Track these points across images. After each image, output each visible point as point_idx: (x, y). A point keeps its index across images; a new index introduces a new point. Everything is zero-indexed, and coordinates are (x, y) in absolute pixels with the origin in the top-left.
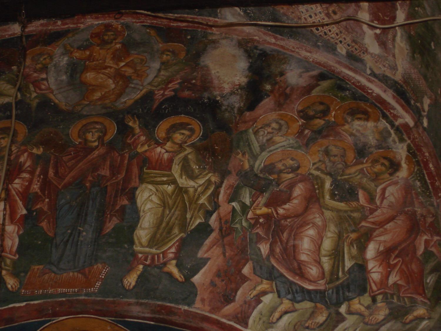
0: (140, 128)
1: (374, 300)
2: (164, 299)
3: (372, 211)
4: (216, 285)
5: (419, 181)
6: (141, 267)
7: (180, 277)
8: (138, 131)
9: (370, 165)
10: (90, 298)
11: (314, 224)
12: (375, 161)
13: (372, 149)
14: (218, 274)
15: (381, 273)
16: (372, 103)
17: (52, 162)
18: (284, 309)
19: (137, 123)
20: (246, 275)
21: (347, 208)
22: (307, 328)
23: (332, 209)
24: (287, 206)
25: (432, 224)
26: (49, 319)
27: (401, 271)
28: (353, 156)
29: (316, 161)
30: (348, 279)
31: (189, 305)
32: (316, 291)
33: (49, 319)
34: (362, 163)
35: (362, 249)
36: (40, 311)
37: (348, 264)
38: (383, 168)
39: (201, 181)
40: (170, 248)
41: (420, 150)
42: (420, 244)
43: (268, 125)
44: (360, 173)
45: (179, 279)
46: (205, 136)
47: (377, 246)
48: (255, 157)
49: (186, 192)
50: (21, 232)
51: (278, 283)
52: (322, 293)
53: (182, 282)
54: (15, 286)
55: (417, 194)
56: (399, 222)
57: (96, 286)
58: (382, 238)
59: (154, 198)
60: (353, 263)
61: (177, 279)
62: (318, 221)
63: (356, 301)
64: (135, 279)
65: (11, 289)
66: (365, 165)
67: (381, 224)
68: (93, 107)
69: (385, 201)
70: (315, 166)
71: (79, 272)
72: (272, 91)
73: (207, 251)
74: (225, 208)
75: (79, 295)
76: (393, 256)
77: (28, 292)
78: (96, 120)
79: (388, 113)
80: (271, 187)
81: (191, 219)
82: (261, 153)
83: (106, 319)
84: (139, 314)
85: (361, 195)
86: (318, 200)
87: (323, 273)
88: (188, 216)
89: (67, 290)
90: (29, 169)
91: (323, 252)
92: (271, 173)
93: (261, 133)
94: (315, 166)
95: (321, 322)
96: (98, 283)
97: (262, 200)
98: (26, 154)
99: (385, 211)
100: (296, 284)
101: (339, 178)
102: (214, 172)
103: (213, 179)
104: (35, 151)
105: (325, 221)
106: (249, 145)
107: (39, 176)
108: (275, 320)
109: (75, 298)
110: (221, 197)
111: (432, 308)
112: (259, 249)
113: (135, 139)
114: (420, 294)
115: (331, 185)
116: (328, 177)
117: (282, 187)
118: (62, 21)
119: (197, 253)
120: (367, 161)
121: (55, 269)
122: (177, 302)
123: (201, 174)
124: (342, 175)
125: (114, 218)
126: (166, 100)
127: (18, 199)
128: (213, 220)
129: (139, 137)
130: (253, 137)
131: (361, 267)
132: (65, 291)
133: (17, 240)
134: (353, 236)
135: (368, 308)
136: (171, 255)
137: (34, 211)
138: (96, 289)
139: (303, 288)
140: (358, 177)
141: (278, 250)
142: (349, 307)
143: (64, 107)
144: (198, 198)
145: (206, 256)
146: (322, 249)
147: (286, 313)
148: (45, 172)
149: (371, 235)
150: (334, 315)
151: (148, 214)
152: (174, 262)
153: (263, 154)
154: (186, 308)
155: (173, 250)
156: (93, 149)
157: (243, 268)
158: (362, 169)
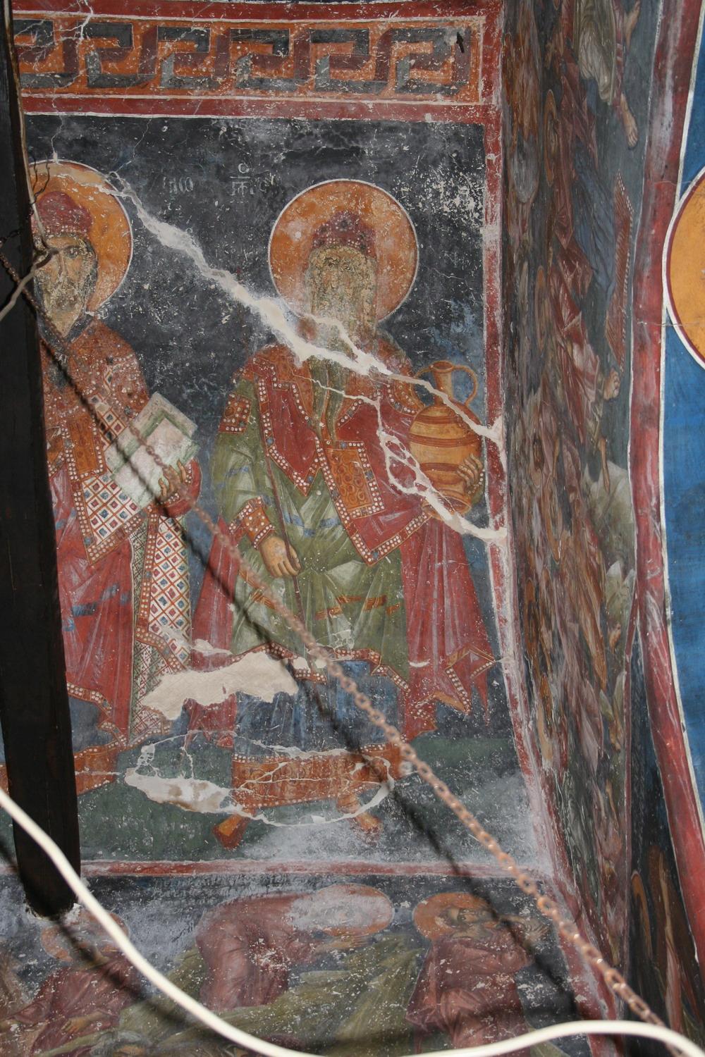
26: (663, 330)
33: (663, 330)
83: (678, 204)
84: (666, 124)
118: (489, 151)
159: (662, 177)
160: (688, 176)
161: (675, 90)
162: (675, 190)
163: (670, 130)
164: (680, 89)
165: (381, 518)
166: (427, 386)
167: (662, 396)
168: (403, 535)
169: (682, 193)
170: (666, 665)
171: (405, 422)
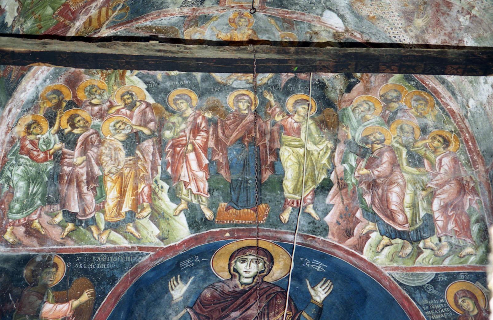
0: (275, 101)
1: (440, 240)
3: (435, 175)
4: (340, 224)
5: (463, 155)
6: (291, 208)
8: (273, 103)
9: (431, 141)
11: (398, 184)
12: (434, 138)
13: (431, 129)
14: (341, 216)
15: (443, 221)
16: (429, 92)
17: (219, 124)
18: (384, 243)
19: (272, 97)
21: (418, 173)
22: (400, 257)
23: (408, 173)
24: (379, 169)
25: (473, 187)
27: (456, 221)
28: (419, 134)
29: (396, 135)
30: (422, 225)
31: (324, 236)
32: (403, 232)
34: (425, 139)
35: (430, 203)
37: (422, 214)
38: (439, 144)
39: (321, 147)
40: (307, 195)
41: (462, 132)
42: (466, 202)
43: (361, 105)
44: (424, 146)
45: (316, 218)
46: (319, 111)
47: (439, 202)
48: (355, 130)
49: (312, 154)
50: (208, 178)
52: (408, 232)
55: (462, 165)
56: (452, 185)
58: (442, 196)
59: (291, 157)
60: (425, 213)
62: (400, 181)
63: (428, 240)
64: (288, 217)
66: (428, 141)
67: (441, 186)
68: (239, 82)
69: (442, 168)
70: (396, 140)
71: (251, 209)
72: (361, 79)
73: (331, 200)
74: (340, 168)
76: (450, 210)
78: (244, 92)
79: (440, 101)
80: (368, 154)
81: (318, 174)
82: (359, 127)
85: (426, 162)
86: (399, 165)
87: (407, 218)
88: (316, 173)
90: (204, 129)
91: (406, 205)
92: (367, 143)
93: (357, 111)
94: (396, 140)
95: (408, 253)
97: (363, 163)
98: (201, 117)
99: (443, 176)
100: (390, 226)
101: (411, 150)
102: (329, 141)
103: (329, 145)
104: (206, 115)
105: (404, 181)
106: (350, 120)
107: (213, 135)
108: (379, 250)
110: (336, 159)
111: (477, 248)
112: (365, 200)
113: (273, 111)
114: (469, 238)
115: (407, 155)
116: (404, 149)
117: (375, 154)
119: (325, 200)
120: (428, 138)
121: (235, 206)
123: (320, 141)
124: (413, 148)
125: (268, 171)
126: (290, 80)
127: (201, 151)
128: (333, 177)
129: (275, 108)
130: (351, 114)
131: (430, 217)
133: (207, 184)
134: (424, 193)
135: (437, 245)
136: (309, 201)
137: (213, 162)
139: (395, 229)
140: (424, 150)
141: (377, 201)
142: (425, 244)
143: (220, 80)
144: (321, 160)
145: (331, 203)
146: (404, 201)
147: (387, 245)
148: (216, 132)
149: (435, 194)
150: (415, 248)
151: (290, 169)
152: (311, 206)
153: (360, 127)
154: (323, 238)
155: (309, 197)
156: (245, 116)
157: (355, 213)
158: (426, 144)
165: (70, 12)
166: (120, 7)
168: (64, 21)
171: (106, 5)
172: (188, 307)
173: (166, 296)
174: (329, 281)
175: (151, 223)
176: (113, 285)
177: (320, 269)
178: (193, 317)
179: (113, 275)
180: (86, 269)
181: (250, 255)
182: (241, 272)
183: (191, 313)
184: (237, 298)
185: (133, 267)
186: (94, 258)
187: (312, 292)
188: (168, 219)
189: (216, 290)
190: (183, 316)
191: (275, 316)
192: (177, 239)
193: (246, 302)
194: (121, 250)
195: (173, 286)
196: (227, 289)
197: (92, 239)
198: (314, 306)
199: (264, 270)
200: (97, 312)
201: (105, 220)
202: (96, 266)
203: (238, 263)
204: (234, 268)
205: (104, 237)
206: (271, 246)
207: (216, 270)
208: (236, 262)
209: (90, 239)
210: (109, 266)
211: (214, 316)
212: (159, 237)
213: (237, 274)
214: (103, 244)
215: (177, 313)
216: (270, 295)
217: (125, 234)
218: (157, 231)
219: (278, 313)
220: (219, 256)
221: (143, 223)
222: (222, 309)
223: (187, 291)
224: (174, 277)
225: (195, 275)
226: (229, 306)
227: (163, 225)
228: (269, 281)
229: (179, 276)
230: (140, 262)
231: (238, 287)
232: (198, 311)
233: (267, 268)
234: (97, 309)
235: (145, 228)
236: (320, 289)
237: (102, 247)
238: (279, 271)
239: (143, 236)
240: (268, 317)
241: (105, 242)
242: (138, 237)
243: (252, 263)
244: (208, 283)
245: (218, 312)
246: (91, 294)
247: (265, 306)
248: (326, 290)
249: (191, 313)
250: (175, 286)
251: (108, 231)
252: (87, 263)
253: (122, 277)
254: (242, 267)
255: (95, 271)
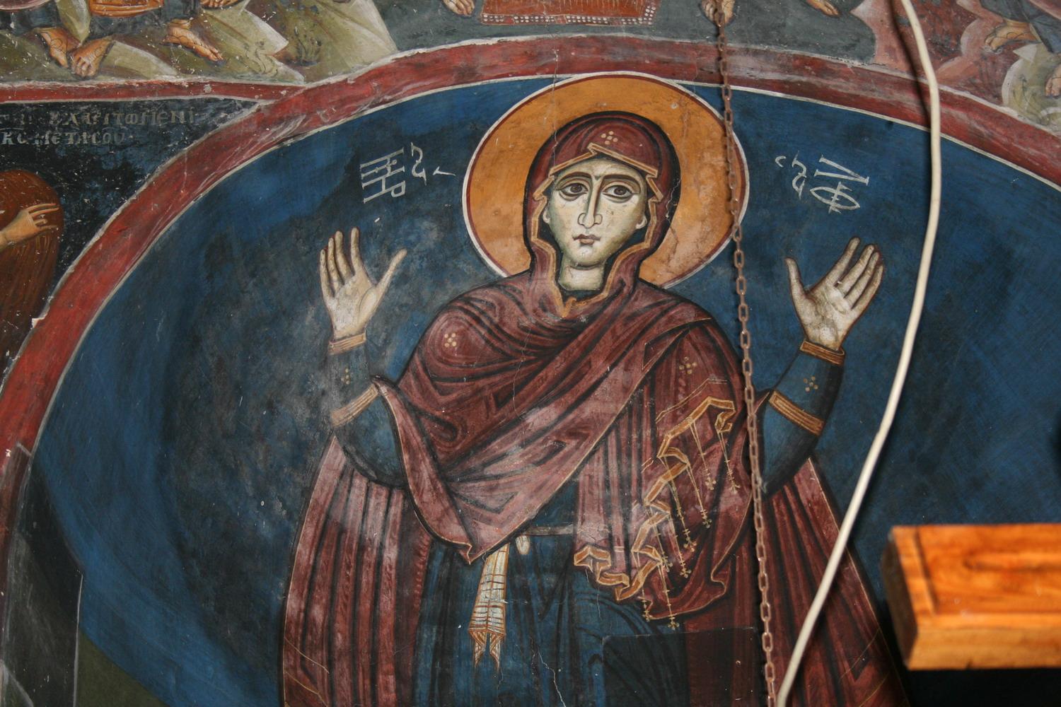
2: (804, 45)
7: (826, 6)
10: (640, 37)
20: (968, 9)
26: (550, 76)
31: (861, 58)
33: (550, 76)
36: (532, 56)
45: (826, 9)
51: (1039, 26)
53: (836, 17)
54: (464, 5)
57: (646, 15)
61: (821, 10)
65: (456, 10)
75: (613, 30)
77: (499, 19)
84: (753, 73)
89: (586, 19)
96: (650, 9)
109: (606, 35)
122: (832, 50)
132: (581, 19)
138: (648, 21)
154: (857, 63)
159: (702, 70)
160: (700, 91)
161: (785, 82)
162: (687, 80)
163: (747, 76)
164: (787, 86)
167: (485, 82)
169: (684, 86)
170: (244, 157)
172: (384, 379)
173: (311, 312)
174: (870, 250)
175: (256, 18)
176: (126, 191)
177: (842, 200)
178: (399, 420)
179: (126, 164)
180: (30, 148)
181: (600, 156)
182: (567, 237)
183: (393, 404)
184: (545, 355)
185: (196, 142)
186: (54, 116)
187: (806, 311)
188: (314, 8)
189: (478, 320)
190: (367, 410)
191: (675, 419)
192: (350, 64)
193: (575, 370)
194: (152, 93)
195: (335, 277)
196: (516, 320)
197: (46, 65)
198: (813, 364)
199: (643, 230)
200: (70, 270)
201: (91, 12)
202: (63, 139)
203: (557, 197)
204: (542, 223)
205: (90, 58)
206: (674, 107)
207: (483, 227)
208: (548, 193)
209: (39, 64)
210: (108, 138)
211: (470, 423)
212: (285, 58)
213: (550, 251)
214: (86, 78)
215: (348, 393)
216: (658, 340)
217: (164, 49)
218: (280, 43)
219: (686, 409)
220: (494, 162)
221: (225, 20)
222: (496, 396)
223: (380, 310)
224: (338, 236)
225: (409, 246)
226: (520, 387)
227: (300, 25)
228: (658, 283)
229: (354, 233)
230: (221, 126)
231: (553, 311)
232: (416, 399)
233: (654, 220)
234: (69, 261)
235: (233, 32)
236: (835, 294)
237: (86, 85)
238: (695, 231)
239: (228, 56)
240: (653, 426)
241: (92, 73)
242: (212, 56)
243: (603, 197)
244: (451, 289)
245: (483, 407)
246: (47, 216)
247: (641, 386)
248: (856, 294)
249: (393, 404)
250: (342, 281)
251: (104, 43)
252: (30, 131)
253: (159, 169)
254: (568, 213)
255: (62, 154)
